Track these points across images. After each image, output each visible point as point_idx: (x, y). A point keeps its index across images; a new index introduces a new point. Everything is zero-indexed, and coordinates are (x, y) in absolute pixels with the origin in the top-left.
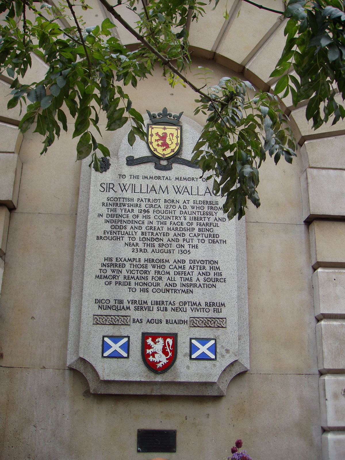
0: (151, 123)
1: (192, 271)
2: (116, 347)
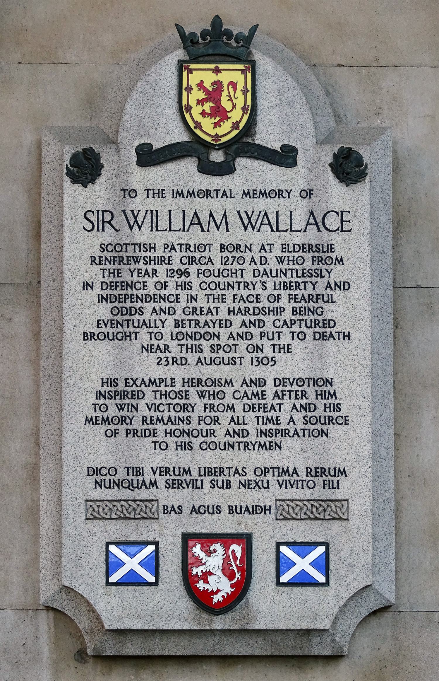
1: (280, 401)
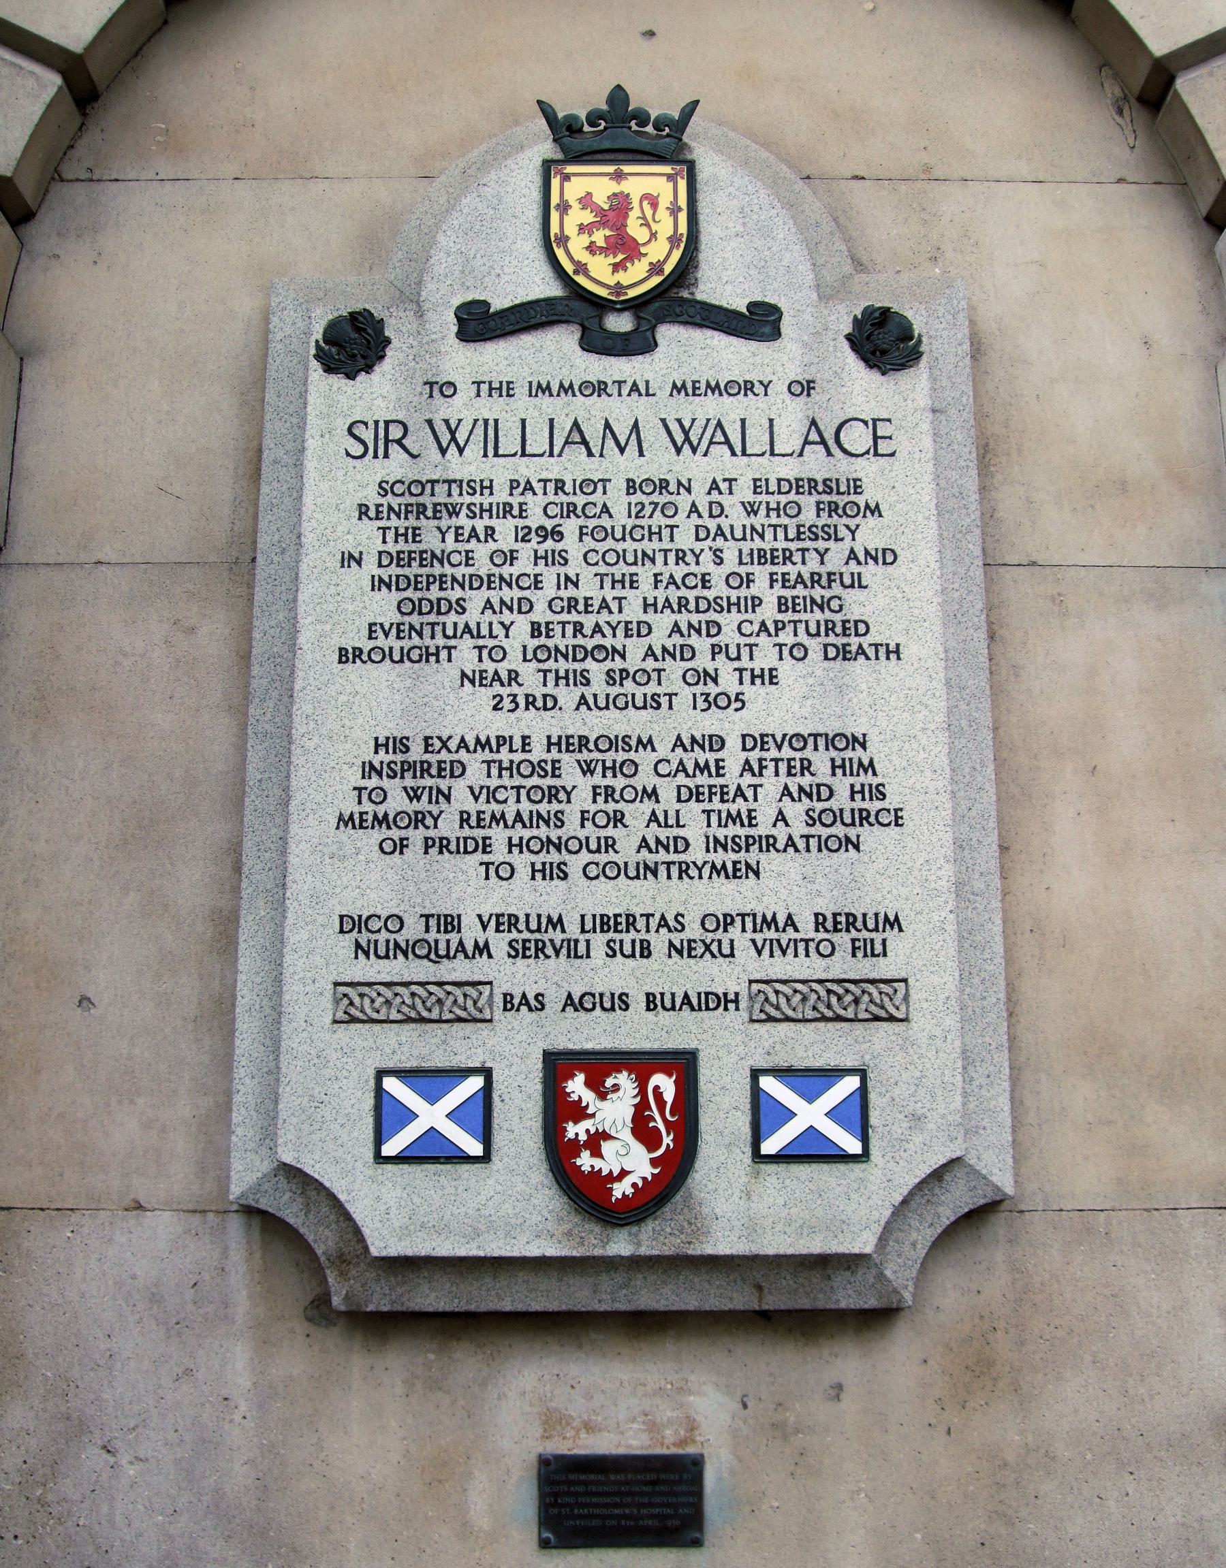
0: (560, 156)
1: (756, 781)
2: (433, 1115)
